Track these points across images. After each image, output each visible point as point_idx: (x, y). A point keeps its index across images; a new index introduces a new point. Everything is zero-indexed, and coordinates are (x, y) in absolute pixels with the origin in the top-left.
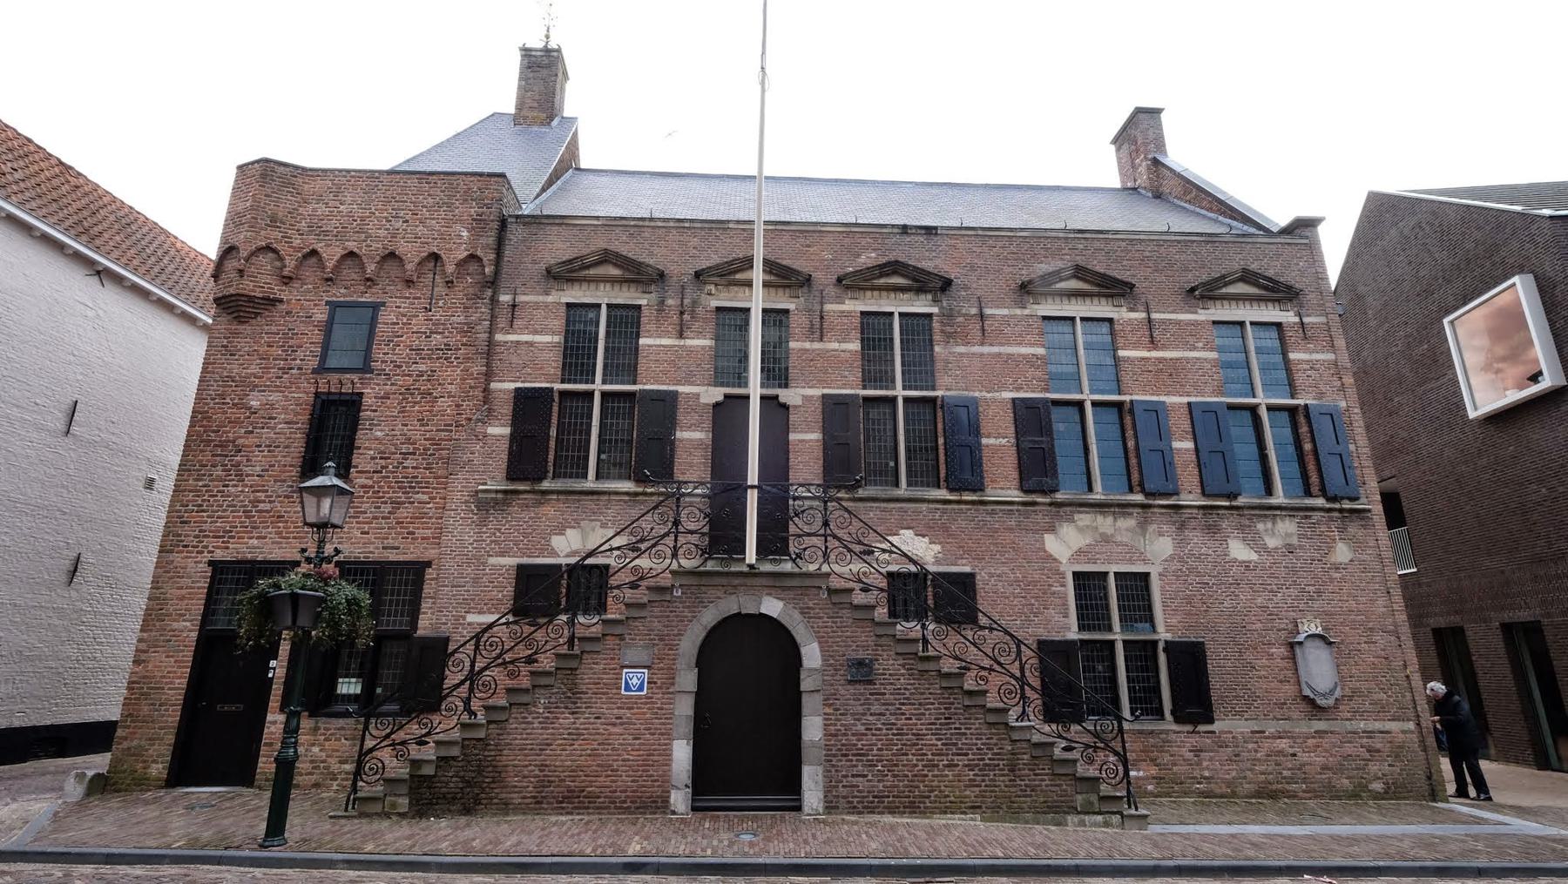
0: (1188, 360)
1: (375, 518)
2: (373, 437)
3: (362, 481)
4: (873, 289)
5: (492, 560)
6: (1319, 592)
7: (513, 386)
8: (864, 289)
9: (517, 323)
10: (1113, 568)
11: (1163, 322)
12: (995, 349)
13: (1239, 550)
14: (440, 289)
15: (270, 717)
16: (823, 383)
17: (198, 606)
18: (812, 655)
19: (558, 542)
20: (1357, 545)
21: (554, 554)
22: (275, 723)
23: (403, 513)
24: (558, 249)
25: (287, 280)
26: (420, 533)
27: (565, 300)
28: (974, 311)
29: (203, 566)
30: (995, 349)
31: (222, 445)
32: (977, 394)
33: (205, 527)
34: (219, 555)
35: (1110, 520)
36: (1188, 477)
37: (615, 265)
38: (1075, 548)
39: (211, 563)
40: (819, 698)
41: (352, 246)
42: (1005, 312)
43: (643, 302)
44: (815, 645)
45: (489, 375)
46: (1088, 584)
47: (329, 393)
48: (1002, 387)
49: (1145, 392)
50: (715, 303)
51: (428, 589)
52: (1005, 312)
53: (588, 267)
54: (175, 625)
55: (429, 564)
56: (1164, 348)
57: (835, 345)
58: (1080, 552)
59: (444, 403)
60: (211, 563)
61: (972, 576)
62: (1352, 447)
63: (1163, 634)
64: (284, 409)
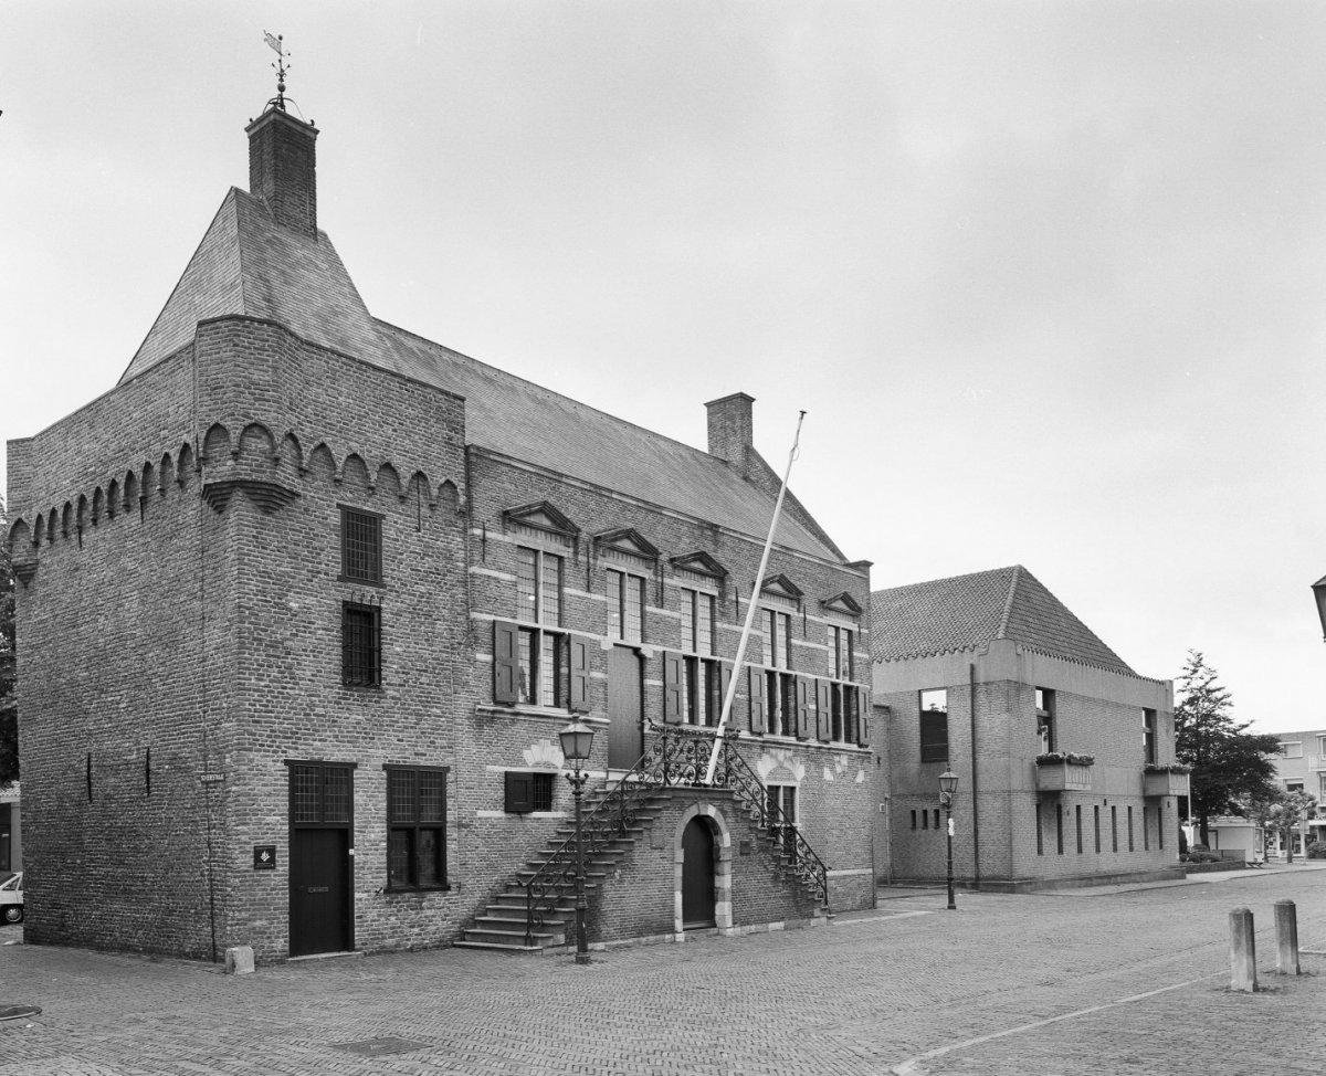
1: (406, 728)
2: (395, 650)
3: (390, 692)
5: (489, 768)
7: (491, 618)
9: (488, 558)
14: (425, 511)
17: (283, 804)
18: (726, 840)
19: (527, 754)
21: (525, 764)
22: (361, 900)
23: (425, 725)
26: (439, 742)
27: (516, 543)
29: (280, 765)
31: (273, 645)
34: (292, 755)
37: (547, 516)
39: (287, 762)
40: (730, 863)
41: (355, 447)
43: (565, 555)
45: (470, 605)
47: (361, 605)
50: (606, 565)
51: (450, 789)
53: (529, 514)
54: (269, 819)
55: (447, 769)
56: (809, 640)
59: (440, 626)
60: (287, 762)
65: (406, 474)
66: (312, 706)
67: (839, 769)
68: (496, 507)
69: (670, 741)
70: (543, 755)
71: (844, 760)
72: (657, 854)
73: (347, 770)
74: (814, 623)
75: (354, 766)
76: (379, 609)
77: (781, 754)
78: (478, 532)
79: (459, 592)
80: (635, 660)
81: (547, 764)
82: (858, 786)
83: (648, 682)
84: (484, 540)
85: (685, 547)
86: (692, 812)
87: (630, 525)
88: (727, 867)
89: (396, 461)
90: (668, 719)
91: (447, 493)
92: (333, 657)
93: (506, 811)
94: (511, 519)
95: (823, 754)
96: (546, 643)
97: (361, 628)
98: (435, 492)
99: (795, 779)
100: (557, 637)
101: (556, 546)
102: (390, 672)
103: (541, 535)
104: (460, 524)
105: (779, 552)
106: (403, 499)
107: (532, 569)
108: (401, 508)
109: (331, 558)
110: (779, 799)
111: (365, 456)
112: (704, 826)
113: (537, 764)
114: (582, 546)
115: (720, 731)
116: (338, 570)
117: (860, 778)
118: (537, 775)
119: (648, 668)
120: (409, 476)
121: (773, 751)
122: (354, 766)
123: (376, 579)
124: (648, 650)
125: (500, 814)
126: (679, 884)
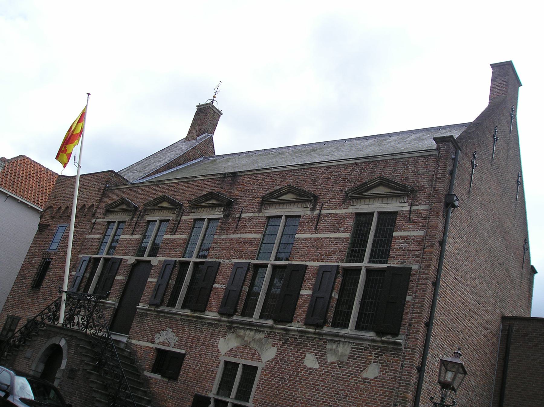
0: (330, 238)
4: (202, 207)
6: (346, 396)
8: (198, 208)
10: (242, 362)
11: (327, 215)
12: (238, 236)
13: (310, 361)
16: (168, 255)
20: (384, 367)
25: (53, 218)
28: (238, 215)
30: (238, 236)
32: (221, 261)
35: (252, 333)
36: (301, 311)
37: (126, 205)
38: (230, 348)
42: (251, 215)
44: (66, 360)
46: (230, 368)
48: (233, 257)
49: (299, 259)
52: (251, 215)
53: (117, 206)
56: (321, 231)
57: (178, 236)
58: (232, 350)
61: (184, 355)
62: (408, 298)
67: (331, 358)
71: (345, 350)
77: (249, 335)
82: (364, 381)
95: (309, 339)
99: (259, 360)
105: (298, 170)
117: (372, 372)
121: (242, 332)
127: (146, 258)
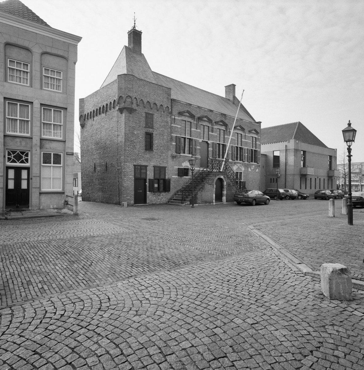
5: (175, 167)
7: (176, 135)
9: (175, 123)
14: (162, 113)
15: (148, 193)
18: (225, 183)
24: (181, 109)
29: (132, 166)
33: (132, 158)
34: (135, 164)
39: (134, 165)
41: (148, 100)
45: (171, 133)
51: (167, 171)
59: (165, 137)
60: (134, 165)
63: (242, 180)
64: (140, 134)
65: (159, 105)
66: (139, 154)
67: (252, 169)
68: (177, 112)
69: (214, 161)
70: (186, 165)
71: (254, 166)
72: (210, 186)
73: (146, 167)
74: (248, 136)
75: (147, 166)
76: (153, 134)
77: (239, 165)
78: (173, 117)
79: (169, 130)
80: (206, 144)
81: (187, 166)
82: (257, 172)
83: (209, 149)
84: (175, 119)
85: (218, 119)
86: (218, 177)
87: (206, 115)
88: (225, 189)
89: (157, 102)
90: (214, 157)
91: (167, 109)
92: (143, 144)
93: (178, 176)
94: (180, 114)
96: (187, 141)
97: (149, 138)
98: (164, 109)
99: (242, 171)
100: (190, 139)
101: (190, 120)
102: (155, 147)
103: (187, 117)
104: (170, 115)
106: (158, 110)
107: (184, 125)
108: (157, 112)
109: (143, 124)
110: (238, 175)
111: (150, 102)
112: (220, 180)
113: (185, 166)
114: (195, 119)
115: (224, 160)
116: (144, 126)
117: (257, 170)
118: (185, 169)
119: (210, 146)
120: (159, 106)
122: (147, 166)
123: (152, 128)
124: (209, 142)
125: (177, 177)
126: (214, 192)
127: (205, 140)
